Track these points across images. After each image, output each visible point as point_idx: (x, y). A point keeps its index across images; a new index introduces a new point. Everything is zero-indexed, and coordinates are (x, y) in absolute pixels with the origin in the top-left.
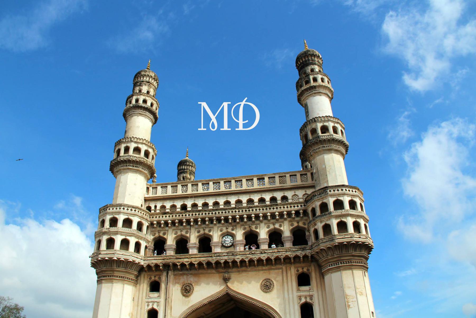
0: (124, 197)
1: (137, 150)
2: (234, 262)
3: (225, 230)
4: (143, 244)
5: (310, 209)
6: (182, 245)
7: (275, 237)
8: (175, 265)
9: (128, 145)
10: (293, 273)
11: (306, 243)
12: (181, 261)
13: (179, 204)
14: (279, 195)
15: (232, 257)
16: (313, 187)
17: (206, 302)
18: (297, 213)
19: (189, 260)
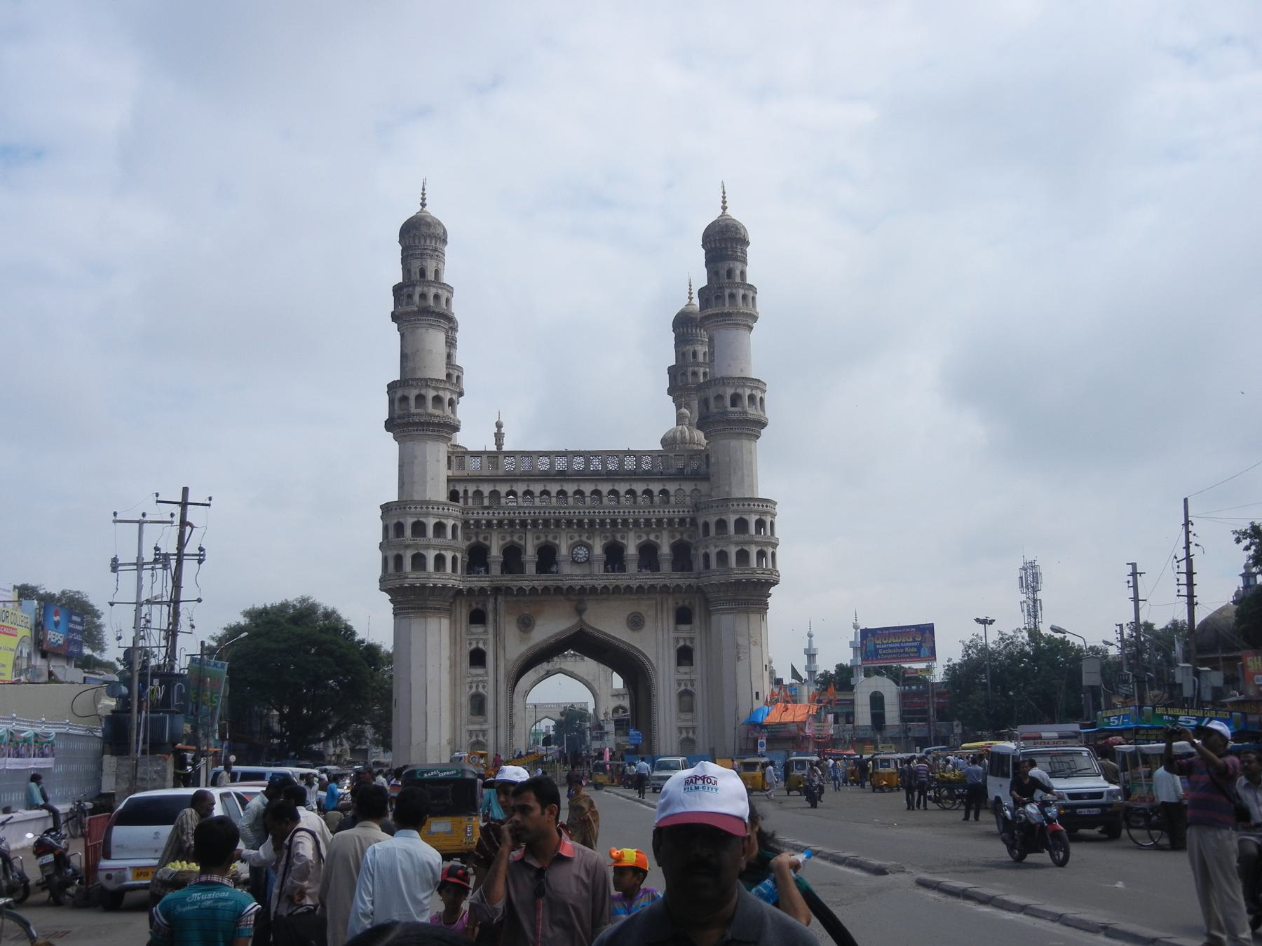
0: (425, 483)
1: (438, 400)
2: (593, 589)
3: (577, 539)
4: (459, 555)
5: (700, 522)
6: (512, 557)
7: (648, 554)
8: (508, 589)
9: (423, 392)
10: (671, 604)
11: (691, 569)
12: (519, 584)
13: (503, 489)
14: (656, 488)
15: (591, 583)
16: (706, 478)
17: (552, 641)
18: (682, 521)
19: (531, 584)
